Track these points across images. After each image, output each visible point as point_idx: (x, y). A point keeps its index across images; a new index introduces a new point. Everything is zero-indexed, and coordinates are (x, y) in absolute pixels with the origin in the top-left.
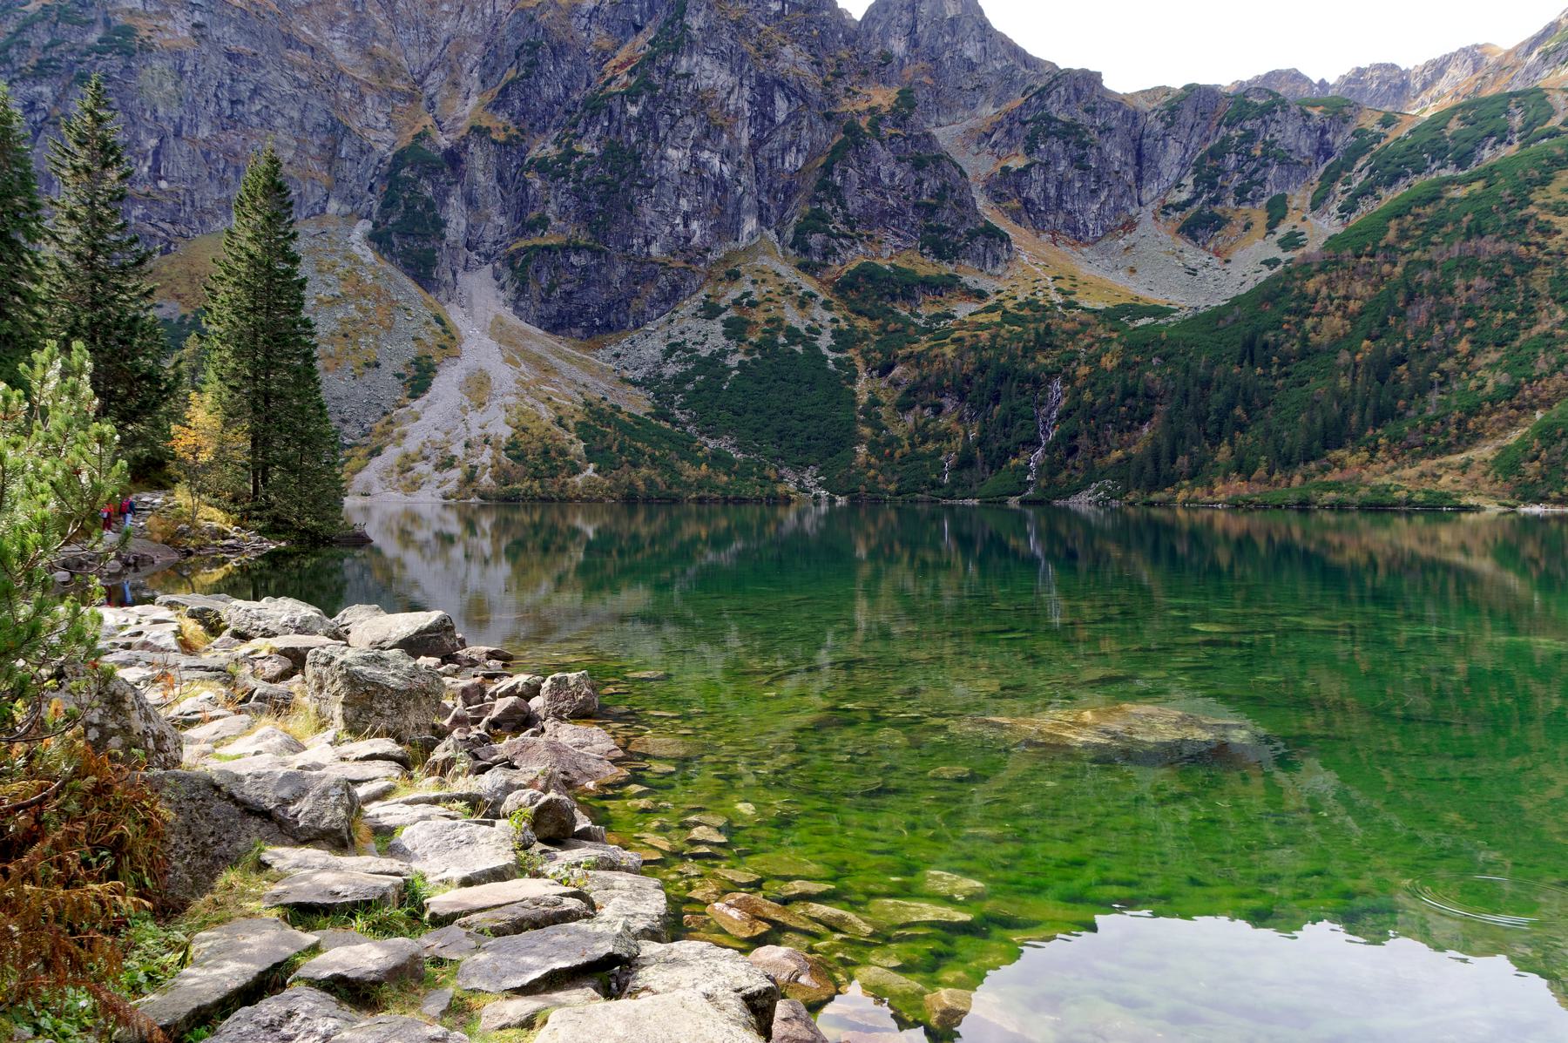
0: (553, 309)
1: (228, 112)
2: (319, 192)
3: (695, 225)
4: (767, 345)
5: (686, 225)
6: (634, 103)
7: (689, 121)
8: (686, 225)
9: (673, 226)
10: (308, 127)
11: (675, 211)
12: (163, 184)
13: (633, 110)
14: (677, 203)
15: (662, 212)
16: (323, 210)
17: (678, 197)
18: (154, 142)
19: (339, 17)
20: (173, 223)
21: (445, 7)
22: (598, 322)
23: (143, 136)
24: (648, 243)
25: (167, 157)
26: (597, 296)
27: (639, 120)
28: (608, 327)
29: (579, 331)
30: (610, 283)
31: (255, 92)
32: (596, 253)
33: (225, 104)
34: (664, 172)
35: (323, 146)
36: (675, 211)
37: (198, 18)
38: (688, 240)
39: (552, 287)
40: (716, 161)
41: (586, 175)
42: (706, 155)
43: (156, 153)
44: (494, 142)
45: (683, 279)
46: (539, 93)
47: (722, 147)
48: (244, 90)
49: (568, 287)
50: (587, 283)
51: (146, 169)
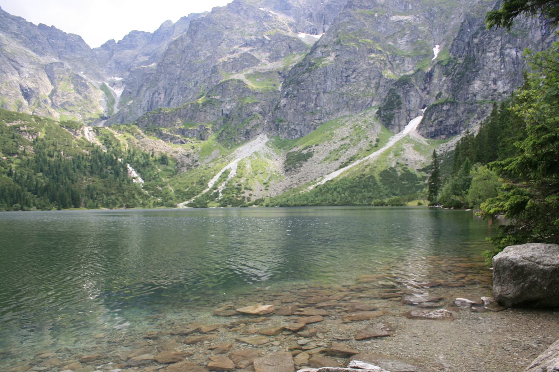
0: (433, 129)
1: (345, 80)
2: (370, 100)
3: (499, 83)
5: (495, 84)
6: (476, 37)
7: (498, 38)
8: (495, 84)
9: (488, 86)
10: (372, 77)
11: (488, 79)
12: (318, 108)
13: (476, 41)
14: (490, 75)
15: (483, 81)
16: (371, 105)
17: (490, 72)
18: (315, 96)
19: (405, 35)
20: (319, 120)
21: (453, 16)
22: (452, 132)
23: (312, 95)
24: (475, 95)
25: (320, 100)
26: (451, 121)
27: (477, 44)
29: (444, 137)
30: (457, 115)
31: (354, 71)
32: (452, 103)
33: (344, 78)
34: (485, 63)
35: (376, 83)
37: (338, 53)
39: (435, 120)
40: (514, 52)
41: (456, 72)
42: (508, 51)
43: (316, 99)
44: (442, 66)
45: (487, 108)
46: (464, 41)
47: (517, 45)
48: (350, 72)
50: (448, 116)
51: (313, 105)
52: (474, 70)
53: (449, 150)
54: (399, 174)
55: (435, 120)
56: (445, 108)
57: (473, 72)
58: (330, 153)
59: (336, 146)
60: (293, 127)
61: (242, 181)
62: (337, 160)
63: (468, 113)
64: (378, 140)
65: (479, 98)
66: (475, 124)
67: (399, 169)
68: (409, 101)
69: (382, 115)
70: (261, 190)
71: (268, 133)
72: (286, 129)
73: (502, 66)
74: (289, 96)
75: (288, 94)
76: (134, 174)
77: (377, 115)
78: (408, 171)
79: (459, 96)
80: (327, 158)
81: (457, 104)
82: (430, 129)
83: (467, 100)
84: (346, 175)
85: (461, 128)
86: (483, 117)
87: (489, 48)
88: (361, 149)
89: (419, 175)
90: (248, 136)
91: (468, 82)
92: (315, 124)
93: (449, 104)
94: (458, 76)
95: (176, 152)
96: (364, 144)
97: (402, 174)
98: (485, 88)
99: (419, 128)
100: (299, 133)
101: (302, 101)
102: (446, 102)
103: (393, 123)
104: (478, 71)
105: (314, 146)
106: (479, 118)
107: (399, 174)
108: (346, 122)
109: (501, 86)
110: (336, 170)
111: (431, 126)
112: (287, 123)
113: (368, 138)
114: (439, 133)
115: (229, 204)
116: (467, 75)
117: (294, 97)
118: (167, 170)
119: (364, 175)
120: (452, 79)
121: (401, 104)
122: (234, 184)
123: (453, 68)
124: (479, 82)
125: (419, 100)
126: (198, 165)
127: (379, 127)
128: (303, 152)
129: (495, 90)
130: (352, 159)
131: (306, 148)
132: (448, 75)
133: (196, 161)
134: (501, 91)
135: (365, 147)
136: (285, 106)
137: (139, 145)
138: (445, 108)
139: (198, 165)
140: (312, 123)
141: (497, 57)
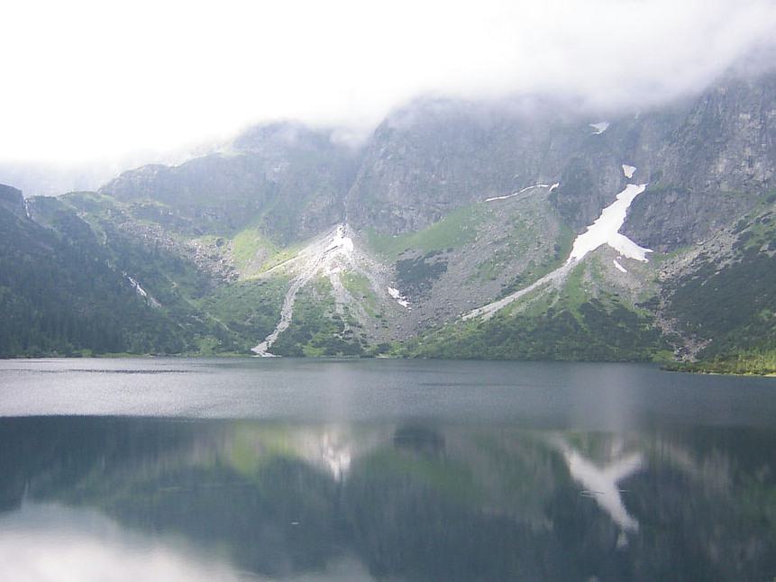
0: (648, 233)
2: (533, 173)
3: (758, 165)
4: (755, 250)
12: (444, 182)
17: (744, 147)
18: (438, 161)
23: (433, 159)
26: (678, 223)
27: (724, 97)
28: (684, 242)
32: (681, 192)
36: (741, 157)
38: (752, 177)
39: (650, 220)
41: (687, 138)
49: (659, 218)
52: (717, 141)
53: (682, 274)
54: (609, 313)
55: (650, 220)
56: (670, 199)
57: (715, 143)
58: (479, 268)
59: (487, 255)
60: (397, 213)
61: (340, 310)
62: (494, 279)
63: (707, 211)
64: (557, 248)
65: (724, 187)
66: (720, 233)
67: (605, 302)
68: (603, 182)
69: (558, 204)
70: (377, 328)
71: (352, 223)
72: (384, 216)
73: (764, 139)
74: (389, 158)
75: (385, 155)
76: (143, 293)
77: (549, 202)
78: (622, 306)
79: (692, 181)
80: (472, 278)
81: (689, 193)
82: (642, 233)
83: (706, 189)
84: (522, 308)
85: (695, 235)
86: (732, 219)
87: (744, 106)
88: (532, 263)
89: (642, 313)
90: (319, 226)
91: (708, 159)
92: (438, 210)
93: (675, 194)
94: (692, 147)
95: (193, 251)
96: (536, 255)
97: (615, 312)
98: (736, 171)
99: (623, 231)
100: (408, 225)
101: (416, 167)
102: (670, 189)
103: (578, 218)
104: (724, 143)
105: (445, 250)
106: (723, 221)
107: (609, 313)
108: (496, 210)
109: (761, 169)
110: (498, 299)
111: (644, 229)
112: (386, 206)
113: (539, 243)
114: (657, 242)
115: (339, 351)
116: (706, 148)
117: (401, 159)
118: (184, 284)
119: (552, 311)
120: (679, 150)
121: (592, 185)
122: (325, 315)
123: (681, 129)
124: (725, 161)
125: (618, 180)
126: (237, 276)
127: (555, 227)
128: (426, 261)
129: (752, 177)
130: (521, 281)
131: (431, 255)
132: (672, 142)
133: (232, 268)
134: (760, 178)
135: (538, 261)
136: (382, 176)
137: (124, 235)
138: (670, 199)
139: (237, 276)
140: (431, 208)
141: (757, 121)
